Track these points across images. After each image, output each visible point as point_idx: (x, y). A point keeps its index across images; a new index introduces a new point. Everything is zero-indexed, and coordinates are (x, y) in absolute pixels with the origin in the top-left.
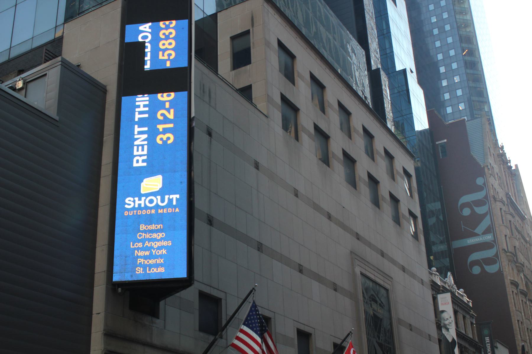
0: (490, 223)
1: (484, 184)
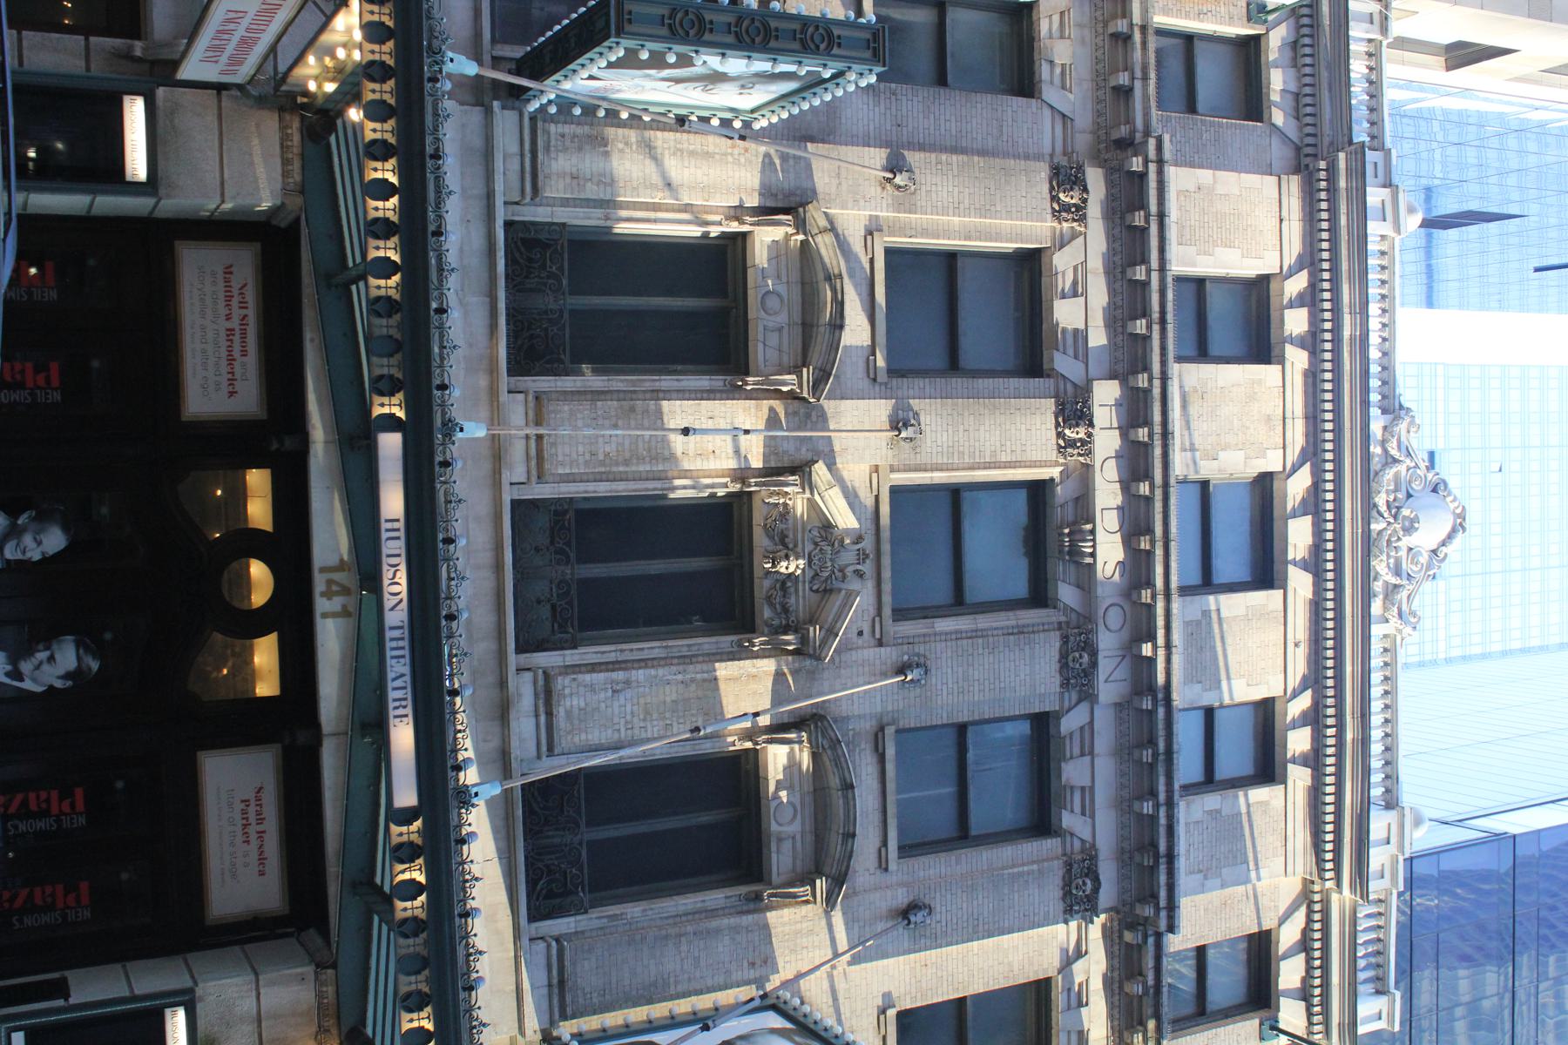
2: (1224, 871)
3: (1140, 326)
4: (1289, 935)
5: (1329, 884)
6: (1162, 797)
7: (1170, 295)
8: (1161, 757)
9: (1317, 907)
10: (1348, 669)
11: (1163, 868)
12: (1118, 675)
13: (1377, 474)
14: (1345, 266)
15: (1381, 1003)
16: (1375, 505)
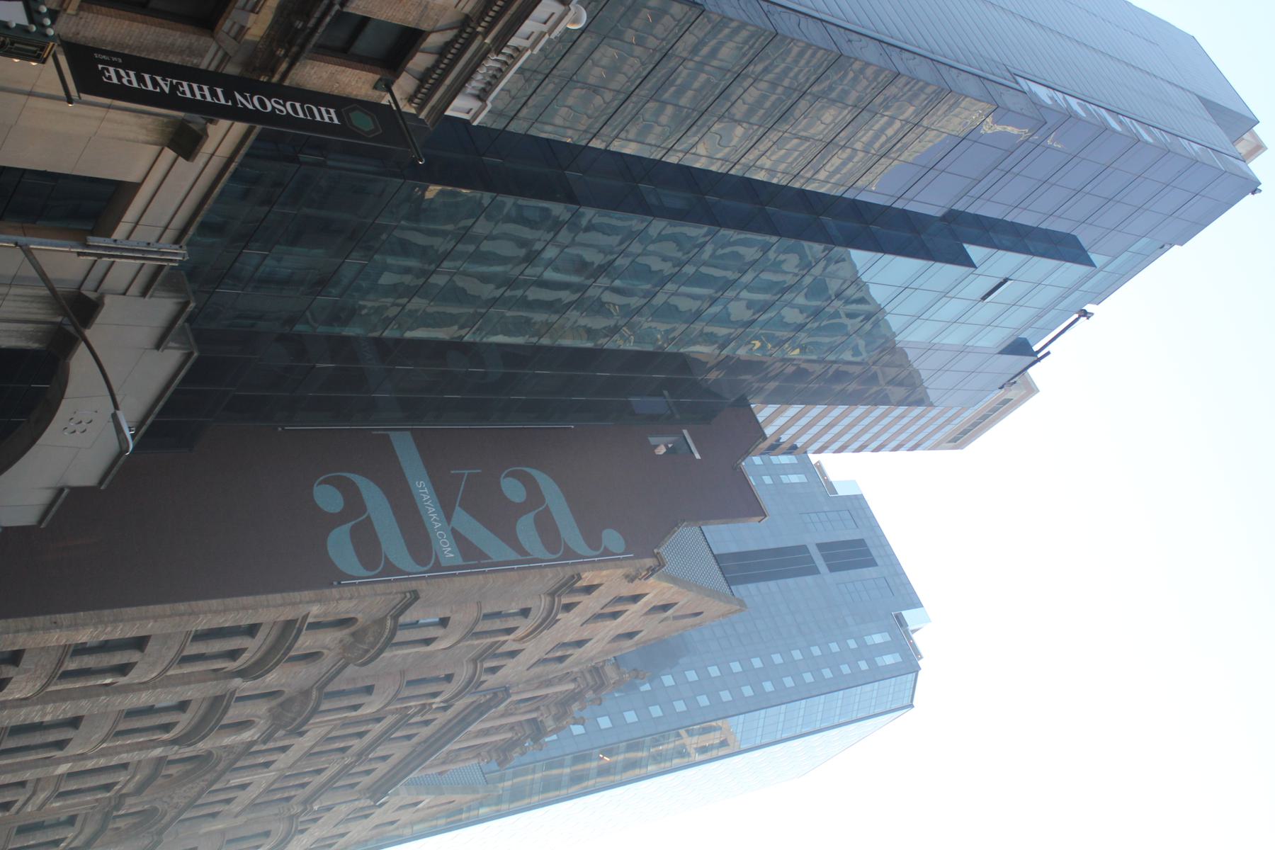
0: (495, 559)
1: (607, 552)
4: (434, 40)
5: (480, 29)
9: (465, 35)
15: (475, 104)
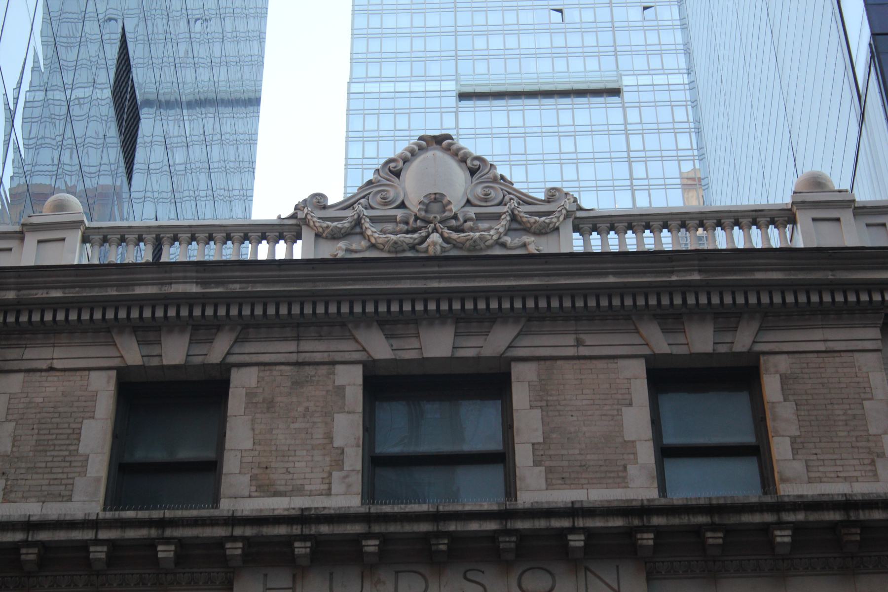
2: (872, 430)
3: (165, 552)
6: (769, 518)
7: (130, 514)
8: (717, 519)
10: (611, 279)
11: (863, 515)
12: (611, 579)
13: (373, 246)
14: (113, 292)
16: (413, 247)
